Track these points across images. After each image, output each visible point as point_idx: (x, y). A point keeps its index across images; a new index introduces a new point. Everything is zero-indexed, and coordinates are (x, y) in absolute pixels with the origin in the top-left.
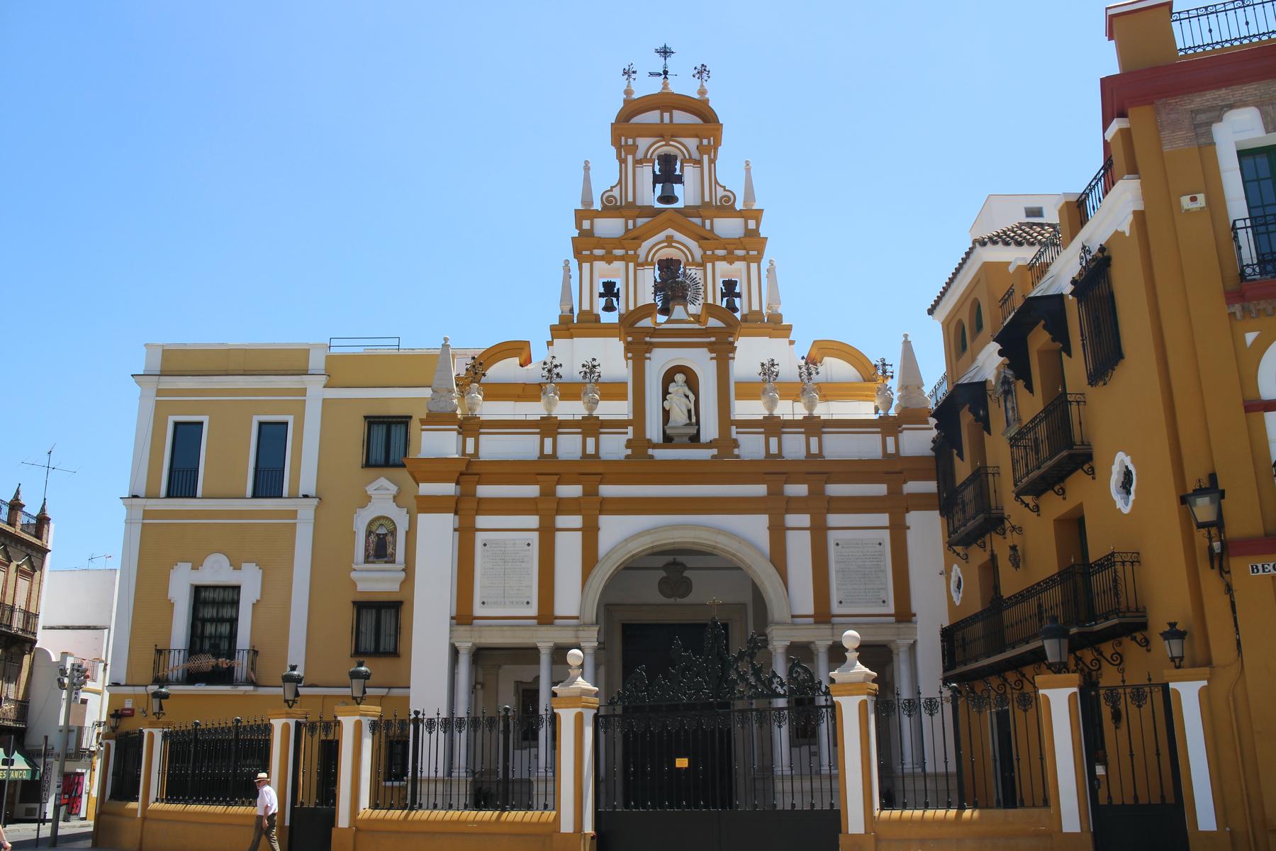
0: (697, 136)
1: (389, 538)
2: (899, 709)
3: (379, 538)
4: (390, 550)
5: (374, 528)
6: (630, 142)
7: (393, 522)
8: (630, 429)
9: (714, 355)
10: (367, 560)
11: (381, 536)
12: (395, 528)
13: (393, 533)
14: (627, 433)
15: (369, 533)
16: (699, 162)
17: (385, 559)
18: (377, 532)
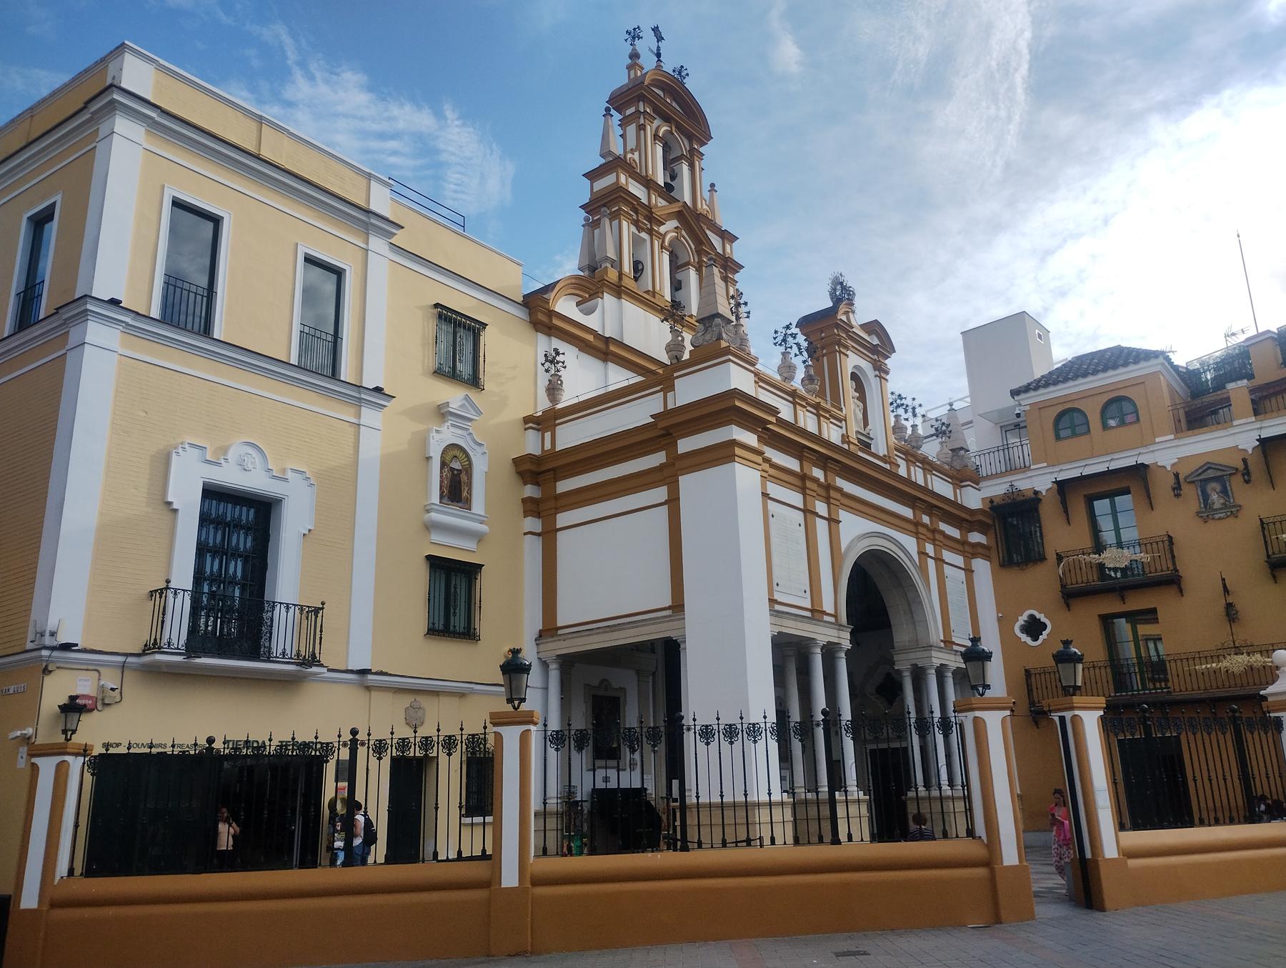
0: (690, 137)
1: (464, 477)
2: (570, 741)
3: (453, 474)
4: (465, 494)
5: (448, 458)
6: (648, 110)
7: (467, 456)
8: (844, 422)
9: (877, 373)
10: (441, 497)
11: (456, 472)
12: (470, 464)
13: (468, 469)
14: (841, 427)
15: (443, 464)
16: (692, 166)
17: (460, 505)
18: (452, 465)
